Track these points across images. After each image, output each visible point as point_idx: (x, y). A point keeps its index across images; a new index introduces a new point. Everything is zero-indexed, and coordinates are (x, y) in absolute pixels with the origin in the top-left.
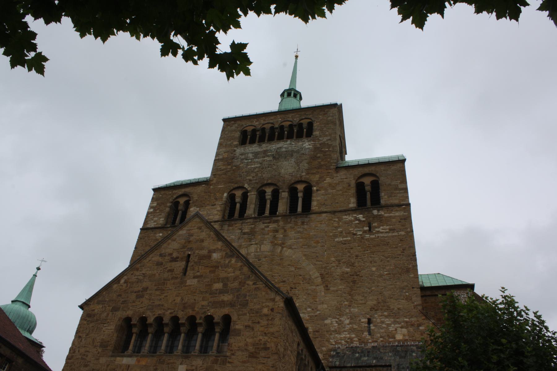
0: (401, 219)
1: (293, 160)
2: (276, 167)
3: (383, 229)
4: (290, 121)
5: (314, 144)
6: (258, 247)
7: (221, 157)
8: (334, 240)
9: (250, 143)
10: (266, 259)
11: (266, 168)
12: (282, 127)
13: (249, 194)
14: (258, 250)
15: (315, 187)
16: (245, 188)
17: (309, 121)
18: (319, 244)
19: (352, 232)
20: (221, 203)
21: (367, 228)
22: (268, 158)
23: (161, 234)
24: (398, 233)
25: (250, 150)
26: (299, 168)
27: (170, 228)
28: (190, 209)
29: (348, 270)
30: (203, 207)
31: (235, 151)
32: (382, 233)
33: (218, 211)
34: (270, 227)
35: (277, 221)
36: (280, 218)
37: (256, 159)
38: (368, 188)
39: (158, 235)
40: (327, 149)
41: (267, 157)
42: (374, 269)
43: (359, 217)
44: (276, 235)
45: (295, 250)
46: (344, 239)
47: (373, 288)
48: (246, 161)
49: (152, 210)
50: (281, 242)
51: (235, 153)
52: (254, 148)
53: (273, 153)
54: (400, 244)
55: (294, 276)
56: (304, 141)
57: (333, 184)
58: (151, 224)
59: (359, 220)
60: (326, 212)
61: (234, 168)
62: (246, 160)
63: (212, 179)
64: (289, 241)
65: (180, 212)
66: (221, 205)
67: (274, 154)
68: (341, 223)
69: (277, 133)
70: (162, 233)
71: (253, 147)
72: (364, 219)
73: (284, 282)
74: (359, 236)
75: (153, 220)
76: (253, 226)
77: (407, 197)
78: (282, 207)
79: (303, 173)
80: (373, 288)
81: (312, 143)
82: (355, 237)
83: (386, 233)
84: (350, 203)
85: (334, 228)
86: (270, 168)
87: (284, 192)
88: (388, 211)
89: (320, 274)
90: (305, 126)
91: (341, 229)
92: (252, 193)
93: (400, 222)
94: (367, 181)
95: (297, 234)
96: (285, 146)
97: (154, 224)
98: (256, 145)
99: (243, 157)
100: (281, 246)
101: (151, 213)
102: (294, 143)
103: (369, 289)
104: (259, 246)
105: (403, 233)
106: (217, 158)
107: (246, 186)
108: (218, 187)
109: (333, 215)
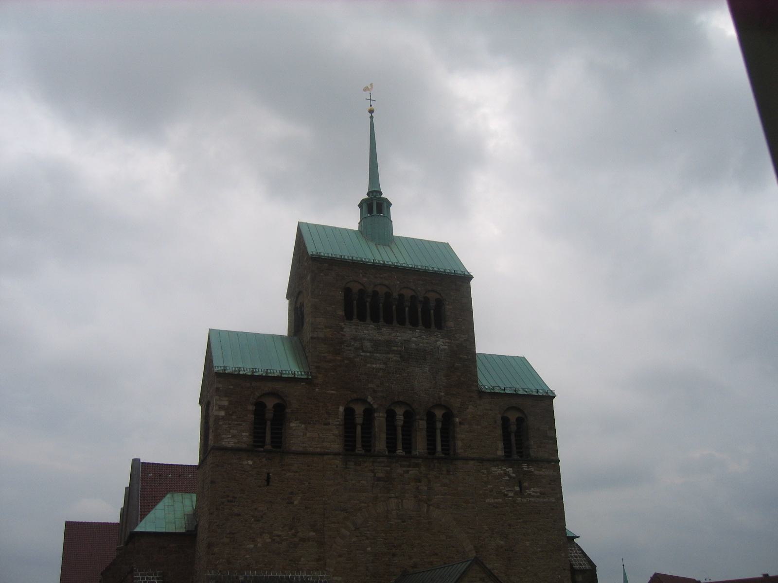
0: (551, 481)
1: (426, 367)
2: (406, 375)
3: (533, 492)
4: (412, 289)
5: (449, 344)
6: (399, 503)
7: (321, 335)
8: (485, 501)
9: (504, 451)
10: (412, 521)
11: (393, 373)
12: (401, 296)
13: (376, 415)
14: (401, 508)
15: (457, 417)
16: (369, 403)
17: (438, 297)
18: (470, 505)
19: (503, 491)
20: (338, 423)
21: (517, 489)
22: (393, 355)
23: (250, 462)
24: (549, 499)
25: (365, 334)
26: (436, 382)
27: (264, 454)
28: (290, 423)
29: (502, 543)
30: (309, 423)
31: (342, 328)
32: (533, 496)
33: (334, 435)
34: (410, 472)
35: (417, 465)
36: (420, 461)
37: (377, 353)
38: (513, 428)
39: (246, 462)
40: (466, 357)
41: (392, 354)
42: (528, 543)
43: (508, 471)
44: (419, 486)
45: (443, 510)
46: (496, 500)
47: (529, 568)
48: (362, 354)
49: (222, 413)
50: (425, 497)
51: (342, 333)
52: (371, 332)
53: (399, 349)
54: (551, 514)
55: (447, 547)
56: (437, 336)
57: (477, 417)
58: (228, 440)
59: (509, 475)
60: (473, 459)
61: (346, 362)
62: (363, 351)
63: (314, 374)
64: (436, 497)
65: (269, 423)
66: (337, 426)
67: (400, 351)
68: (490, 478)
69: (394, 307)
70: (252, 460)
71: (369, 328)
72: (514, 475)
73: (436, 554)
74: (511, 499)
75: (230, 432)
76: (389, 469)
77: (556, 451)
78: (420, 446)
79: (441, 392)
80: (529, 568)
81: (447, 341)
82: (507, 499)
83: (538, 497)
84: (498, 449)
85: (483, 484)
86: (398, 375)
87: (422, 419)
88: (537, 467)
89: (475, 547)
90: (432, 304)
91: (491, 486)
92: (381, 415)
93: (550, 484)
94: (513, 416)
95: (444, 488)
96: (414, 339)
97: (233, 440)
98: (373, 326)
99: (357, 344)
100: (426, 503)
101: (223, 418)
102: (424, 337)
103: (524, 568)
104: (400, 501)
105: (553, 500)
106: (315, 336)
107: (370, 399)
108: (328, 392)
109: (481, 464)
